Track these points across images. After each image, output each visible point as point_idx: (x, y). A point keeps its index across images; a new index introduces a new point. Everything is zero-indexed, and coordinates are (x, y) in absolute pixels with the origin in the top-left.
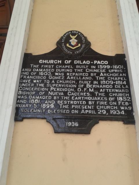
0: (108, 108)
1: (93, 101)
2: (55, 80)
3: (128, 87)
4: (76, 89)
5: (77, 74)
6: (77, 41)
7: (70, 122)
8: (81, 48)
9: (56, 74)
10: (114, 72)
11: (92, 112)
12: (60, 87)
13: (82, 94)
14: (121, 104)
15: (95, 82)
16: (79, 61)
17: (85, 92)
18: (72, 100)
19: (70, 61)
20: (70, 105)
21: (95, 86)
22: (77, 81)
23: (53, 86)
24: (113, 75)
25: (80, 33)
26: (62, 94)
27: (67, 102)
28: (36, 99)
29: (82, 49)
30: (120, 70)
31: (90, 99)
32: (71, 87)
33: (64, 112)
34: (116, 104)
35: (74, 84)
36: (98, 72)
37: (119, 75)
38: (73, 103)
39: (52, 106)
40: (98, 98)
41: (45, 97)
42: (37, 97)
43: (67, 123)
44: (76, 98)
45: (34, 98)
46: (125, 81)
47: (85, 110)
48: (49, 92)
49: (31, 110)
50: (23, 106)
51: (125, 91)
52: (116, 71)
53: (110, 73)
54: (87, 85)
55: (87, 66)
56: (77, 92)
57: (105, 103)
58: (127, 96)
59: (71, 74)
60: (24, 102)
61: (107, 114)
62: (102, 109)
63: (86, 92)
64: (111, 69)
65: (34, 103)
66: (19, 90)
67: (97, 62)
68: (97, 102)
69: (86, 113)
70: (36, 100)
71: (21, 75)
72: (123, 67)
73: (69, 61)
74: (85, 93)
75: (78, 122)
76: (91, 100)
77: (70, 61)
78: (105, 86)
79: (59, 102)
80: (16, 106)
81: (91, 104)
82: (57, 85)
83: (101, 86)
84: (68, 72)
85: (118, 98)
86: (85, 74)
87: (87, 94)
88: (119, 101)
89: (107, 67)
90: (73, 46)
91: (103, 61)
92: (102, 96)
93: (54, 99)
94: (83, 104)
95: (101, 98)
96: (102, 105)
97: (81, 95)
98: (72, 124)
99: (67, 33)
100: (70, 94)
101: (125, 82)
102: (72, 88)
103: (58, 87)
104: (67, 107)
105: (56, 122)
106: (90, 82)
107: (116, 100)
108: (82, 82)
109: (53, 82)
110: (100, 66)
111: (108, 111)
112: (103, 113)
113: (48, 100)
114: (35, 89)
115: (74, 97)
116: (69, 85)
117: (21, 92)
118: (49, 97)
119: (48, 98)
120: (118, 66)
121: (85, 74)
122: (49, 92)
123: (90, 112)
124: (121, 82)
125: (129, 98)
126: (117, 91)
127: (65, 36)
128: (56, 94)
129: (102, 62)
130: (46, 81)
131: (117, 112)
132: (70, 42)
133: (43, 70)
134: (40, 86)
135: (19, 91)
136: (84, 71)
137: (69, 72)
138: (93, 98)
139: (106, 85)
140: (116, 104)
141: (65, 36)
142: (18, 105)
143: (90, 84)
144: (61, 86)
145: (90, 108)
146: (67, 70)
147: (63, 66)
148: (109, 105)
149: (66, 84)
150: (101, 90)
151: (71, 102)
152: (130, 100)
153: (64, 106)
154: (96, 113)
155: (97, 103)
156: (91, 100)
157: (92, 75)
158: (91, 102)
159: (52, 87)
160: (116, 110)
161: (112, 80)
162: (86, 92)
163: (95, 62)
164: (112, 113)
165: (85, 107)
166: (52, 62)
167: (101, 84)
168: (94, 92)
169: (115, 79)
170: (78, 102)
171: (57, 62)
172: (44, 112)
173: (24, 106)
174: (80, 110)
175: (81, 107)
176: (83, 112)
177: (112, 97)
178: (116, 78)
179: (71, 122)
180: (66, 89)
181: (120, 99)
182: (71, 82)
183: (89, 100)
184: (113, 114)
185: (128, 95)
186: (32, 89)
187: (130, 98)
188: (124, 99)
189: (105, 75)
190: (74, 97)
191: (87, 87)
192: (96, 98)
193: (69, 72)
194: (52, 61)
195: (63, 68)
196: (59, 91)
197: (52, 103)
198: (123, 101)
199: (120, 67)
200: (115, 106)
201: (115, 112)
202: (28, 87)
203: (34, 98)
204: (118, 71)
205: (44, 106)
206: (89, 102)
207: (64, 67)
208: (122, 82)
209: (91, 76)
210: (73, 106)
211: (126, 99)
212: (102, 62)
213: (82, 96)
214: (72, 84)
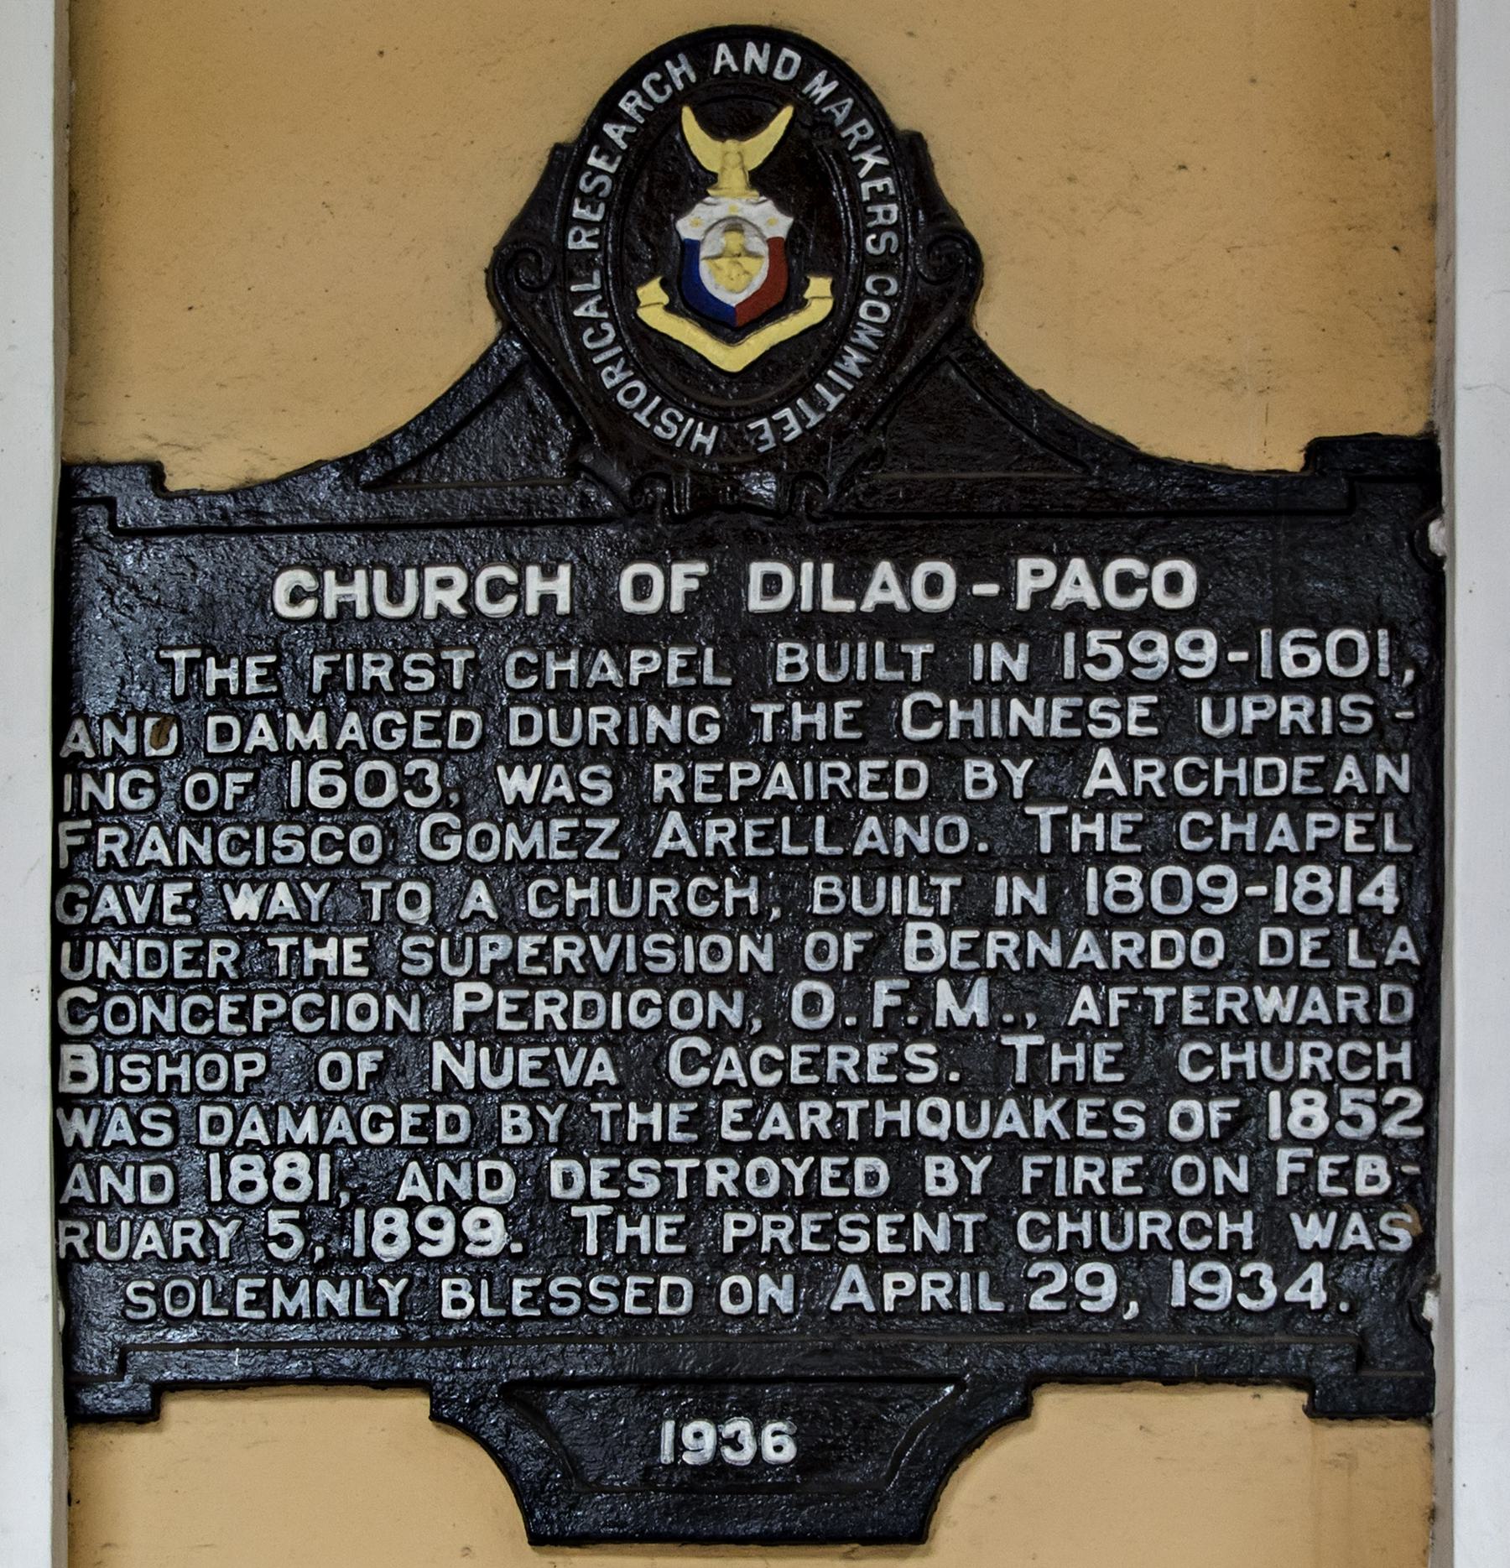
0: (1153, 1238)
1: (973, 1148)
3: (1411, 954)
5: (781, 769)
6: (780, 224)
7: (698, 1416)
8: (833, 355)
9: (517, 784)
10: (1266, 738)
11: (954, 1296)
12: (567, 980)
13: (840, 1060)
14: (1303, 1181)
15: (1014, 892)
16: (807, 567)
17: (876, 1035)
18: (727, 1148)
19: (686, 576)
20: (701, 1208)
21: (1014, 939)
22: (786, 876)
23: (484, 969)
24: (1249, 775)
26: (602, 1068)
27: (668, 1174)
28: (290, 1145)
29: (853, 360)
30: (1346, 701)
31: (940, 1131)
33: (629, 1308)
34: (1241, 1183)
35: (742, 922)
36: (1057, 730)
37: (1324, 774)
38: (732, 1191)
39: (490, 1234)
40: (1039, 1103)
41: (396, 1120)
42: (298, 1121)
43: (669, 1427)
44: (777, 1122)
45: (261, 1135)
46: (1390, 857)
47: (874, 1264)
48: (441, 1052)
49: (242, 1296)
50: (142, 1247)
51: (1373, 1004)
52: (1292, 712)
54: (912, 928)
55: (918, 651)
56: (779, 1030)
57: (1122, 1166)
58: (1394, 1068)
59: (702, 772)
61: (1134, 1305)
62: (1073, 1255)
64: (1231, 681)
65: (271, 1201)
66: (58, 1038)
68: (1027, 1161)
69: (889, 1306)
71: (58, 816)
72: (1384, 655)
73: (679, 570)
74: (877, 1053)
75: (798, 1418)
76: (956, 1146)
77: (686, 576)
78: (1139, 946)
79: (568, 1181)
80: (65, 1240)
81: (952, 1187)
82: (527, 946)
83: (1086, 937)
84: (665, 750)
85: (1275, 1097)
86: (884, 780)
87: (910, 1054)
88: (1289, 1139)
89: (1175, 661)
90: (727, 324)
91: (1137, 568)
92: (1089, 1087)
93: (508, 1138)
94: (861, 1190)
95: (1068, 1114)
97: (832, 1077)
98: (721, 1441)
99: (630, 80)
100: (703, 1073)
101: (1386, 876)
102: (725, 983)
104: (658, 1234)
106: (945, 894)
107: (1242, 1134)
108: (846, 888)
109: (480, 897)
110: (1093, 636)
111: (1143, 1267)
112: (1086, 1305)
113: (430, 1153)
114: (259, 1013)
115: (747, 1103)
116: (678, 947)
117: (90, 1066)
118: (442, 1112)
119: (425, 1126)
120: (1319, 644)
122: (441, 1052)
123: (934, 1289)
124: (1335, 885)
125: (1402, 1103)
126: (1272, 1003)
127: (608, 148)
128: (525, 1066)
129: (1126, 583)
131: (1252, 1286)
132: (691, 249)
133: (332, 736)
134: (320, 965)
135: (68, 1050)
136: (875, 731)
137: (683, 752)
139: (1149, 922)
140: (1241, 1183)
141: (608, 148)
142: (85, 1230)
143: (948, 924)
145: (940, 1243)
146: (654, 715)
147: (604, 657)
148: (1155, 1189)
149: (640, 925)
150: (1086, 994)
151: (712, 1165)
152: (1418, 1132)
153: (624, 1230)
155: (1029, 1173)
156: (956, 1146)
157: (980, 784)
158: (949, 1173)
159: (473, 975)
160: (1233, 1255)
163: (1031, 575)
164: (1191, 1293)
165: (884, 1232)
166: (451, 599)
168: (998, 1026)
169: (1263, 833)
170: (799, 1173)
171: (510, 601)
173: (157, 1246)
174: (815, 1272)
175: (828, 1231)
176: (850, 1289)
177: (1204, 1092)
179: (718, 1420)
180: (645, 1005)
181: (1299, 1111)
182: (703, 895)
183: (934, 1145)
185: (1404, 1057)
187: (1416, 1100)
188: (1347, 1108)
189: (1149, 773)
190: (747, 1103)
191: (912, 964)
192: (1011, 1106)
193: (683, 752)
194: (440, 590)
196: (561, 1025)
197: (485, 1194)
198: (1327, 1142)
199: (1347, 651)
200: (1233, 1202)
201: (1225, 1287)
202: (164, 987)
203: (261, 1135)
204: (1315, 719)
205: (390, 1239)
206: (931, 1162)
207: (612, 674)
208: (1346, 873)
209: (967, 807)
210: (730, 1218)
211: (1369, 1117)
212: (1126, 583)
213: (846, 1089)
214: (716, 922)
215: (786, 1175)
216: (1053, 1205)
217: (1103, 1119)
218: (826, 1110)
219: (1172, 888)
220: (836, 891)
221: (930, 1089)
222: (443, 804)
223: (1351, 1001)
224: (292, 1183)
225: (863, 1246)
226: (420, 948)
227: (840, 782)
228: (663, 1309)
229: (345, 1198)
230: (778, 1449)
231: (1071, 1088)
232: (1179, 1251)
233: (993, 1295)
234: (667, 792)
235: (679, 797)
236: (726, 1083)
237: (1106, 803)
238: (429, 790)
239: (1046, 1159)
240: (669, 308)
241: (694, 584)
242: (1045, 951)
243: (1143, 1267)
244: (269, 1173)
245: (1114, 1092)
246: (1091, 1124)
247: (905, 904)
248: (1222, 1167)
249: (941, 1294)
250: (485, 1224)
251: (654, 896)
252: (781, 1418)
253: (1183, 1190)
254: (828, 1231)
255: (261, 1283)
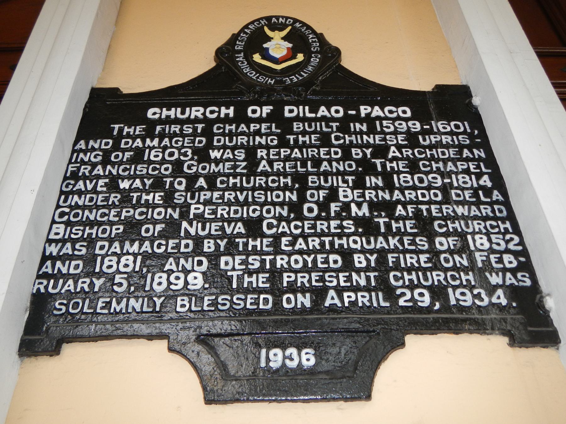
0: (439, 280)
1: (371, 252)
2: (211, 179)
3: (500, 198)
4: (296, 209)
6: (290, 45)
9: (215, 154)
10: (439, 145)
11: (370, 300)
12: (229, 204)
17: (334, 219)
18: (283, 252)
19: (267, 110)
20: (275, 274)
23: (202, 201)
25: (301, 22)
26: (240, 228)
27: (263, 262)
28: (128, 253)
29: (310, 68)
31: (358, 246)
32: (275, 200)
33: (248, 306)
34: (465, 263)
35: (285, 188)
36: (377, 142)
37: (460, 153)
38: (286, 266)
39: (197, 281)
40: (390, 238)
41: (167, 245)
42: (132, 245)
43: (264, 351)
44: (300, 244)
45: (118, 251)
46: (486, 173)
48: (185, 224)
49: (100, 304)
50: (66, 288)
52: (446, 139)
53: (424, 147)
54: (341, 190)
55: (334, 125)
56: (301, 217)
57: (423, 258)
60: (74, 267)
61: (437, 304)
62: (412, 287)
63: (338, 216)
64: (424, 133)
65: (118, 272)
66: (53, 222)
67: (369, 109)
70: (123, 260)
71: (70, 162)
72: (467, 127)
73: (264, 108)
77: (267, 110)
79: (227, 263)
80: (37, 286)
81: (364, 264)
83: (397, 192)
84: (260, 146)
87: (345, 223)
89: (408, 128)
91: (394, 109)
92: (406, 233)
93: (206, 249)
94: (332, 265)
95: (401, 242)
96: (409, 270)
98: (285, 357)
99: (252, 23)
100: (275, 230)
101: (486, 177)
102: (282, 204)
103: (224, 203)
105: (212, 350)
107: (463, 249)
108: (319, 179)
109: (202, 182)
111: (438, 292)
113: (177, 255)
114: (124, 214)
115: (290, 238)
117: (61, 231)
118: (183, 242)
119: (178, 246)
121: (329, 153)
122: (185, 224)
123: (363, 299)
124: (471, 179)
125: (512, 239)
126: (460, 210)
128: (213, 228)
129: (391, 112)
130: (172, 183)
132: (267, 49)
135: (55, 226)
136: (325, 140)
137: (268, 147)
138: (369, 243)
140: (465, 263)
143: (353, 189)
144: (236, 198)
145: (363, 282)
148: (437, 267)
150: (400, 207)
151: (278, 258)
153: (247, 279)
154: (388, 304)
156: (363, 251)
157: (357, 154)
159: (198, 202)
161: (435, 172)
162: (338, 216)
163: (364, 110)
164: (458, 300)
165: (342, 279)
167: (397, 185)
170: (310, 260)
172: (158, 309)
173: (72, 288)
174: (319, 294)
175: (322, 279)
177: (446, 235)
178: (450, 164)
179: (284, 349)
180: (254, 211)
182: (273, 181)
183: (356, 251)
184: (461, 303)
185: (508, 225)
186: (113, 212)
187: (517, 239)
188: (494, 240)
189: (407, 152)
190: (290, 238)
191: (342, 198)
192: (381, 239)
193: (268, 147)
194: (196, 112)
195: (243, 133)
196: (226, 216)
197: (196, 268)
198: (492, 251)
199: (457, 127)
203: (118, 251)
205: (160, 284)
206: (356, 256)
207: (245, 129)
208: (473, 177)
210: (285, 275)
211: (502, 243)
213: (322, 234)
215: (305, 262)
216: (402, 270)
217: (413, 243)
218: (317, 240)
219: (421, 180)
220: (316, 180)
221: (353, 234)
222: (192, 159)
223: (486, 210)
224: (126, 266)
225: (335, 283)
226: (181, 195)
227: (315, 153)
228: (261, 306)
229: (145, 270)
230: (308, 360)
231: (400, 234)
232: (449, 285)
233: (385, 300)
234: (262, 156)
235: (265, 157)
236: (282, 232)
237: (395, 159)
238: (188, 156)
239: (396, 255)
240: (262, 59)
241: (269, 111)
242: (384, 196)
243: (438, 292)
244: (118, 263)
245: (415, 235)
246: (409, 244)
247: (338, 183)
248: (457, 258)
249: (365, 300)
250: (195, 278)
251: (258, 181)
252: (310, 347)
253: (446, 265)
254: (322, 279)
255: (108, 300)
